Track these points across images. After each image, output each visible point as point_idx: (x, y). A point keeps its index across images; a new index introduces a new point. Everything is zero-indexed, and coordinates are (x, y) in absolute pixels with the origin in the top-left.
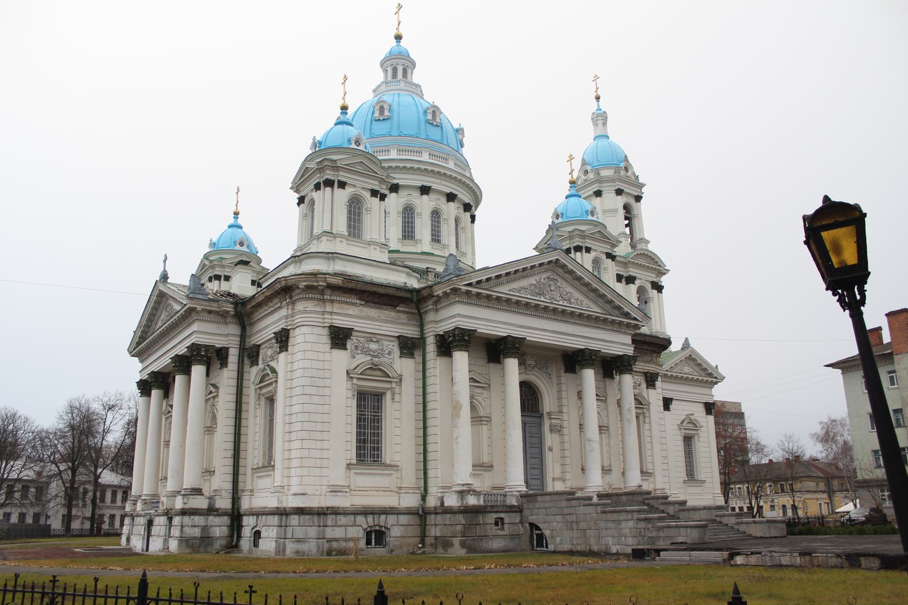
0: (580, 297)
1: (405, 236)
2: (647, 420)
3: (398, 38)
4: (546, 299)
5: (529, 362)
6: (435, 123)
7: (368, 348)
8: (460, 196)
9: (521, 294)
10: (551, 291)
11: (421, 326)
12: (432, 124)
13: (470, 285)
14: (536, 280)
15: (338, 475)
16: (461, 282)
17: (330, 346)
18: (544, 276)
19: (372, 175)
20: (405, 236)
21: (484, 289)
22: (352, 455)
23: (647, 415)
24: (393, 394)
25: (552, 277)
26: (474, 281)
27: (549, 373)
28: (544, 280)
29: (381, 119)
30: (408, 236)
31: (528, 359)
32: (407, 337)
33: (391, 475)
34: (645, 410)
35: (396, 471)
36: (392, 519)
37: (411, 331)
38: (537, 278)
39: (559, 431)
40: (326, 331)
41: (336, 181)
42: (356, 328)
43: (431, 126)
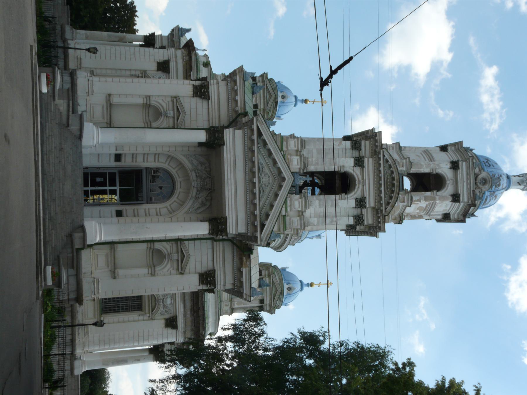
2: (141, 318)
17: (158, 61)
19: (266, 103)
23: (146, 318)
34: (148, 315)
40: (166, 58)
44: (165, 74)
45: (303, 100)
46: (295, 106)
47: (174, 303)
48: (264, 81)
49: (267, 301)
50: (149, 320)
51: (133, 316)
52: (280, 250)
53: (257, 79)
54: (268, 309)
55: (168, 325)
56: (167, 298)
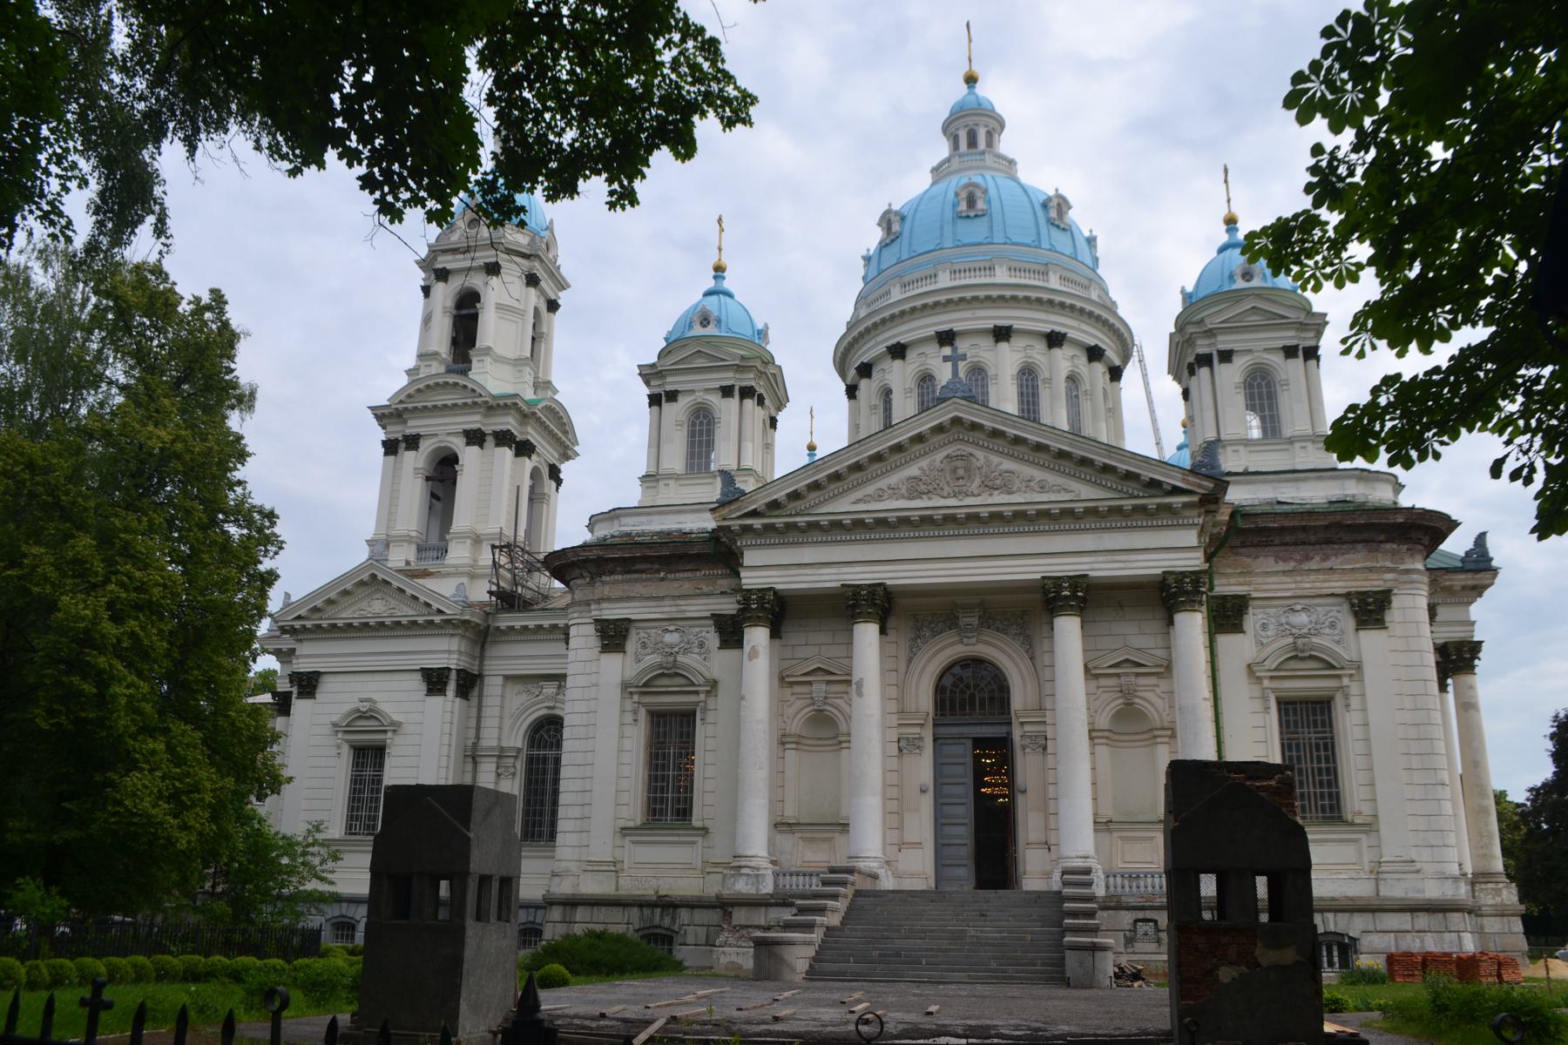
0: (1039, 474)
2: (1355, 702)
3: (971, 80)
5: (963, 621)
6: (972, 214)
8: (1017, 325)
12: (968, 217)
13: (754, 514)
15: (603, 846)
22: (634, 811)
23: (1354, 689)
24: (705, 710)
27: (1028, 632)
31: (961, 615)
32: (724, 616)
33: (694, 843)
34: (1346, 681)
35: (703, 836)
36: (684, 915)
37: (728, 606)
38: (924, 463)
39: (1045, 748)
40: (591, 629)
42: (633, 617)
43: (967, 221)
44: (633, 632)
45: (715, 277)
46: (730, 295)
47: (1303, 601)
48: (661, 372)
49: (1289, 337)
50: (1362, 680)
51: (1347, 723)
52: (1126, 335)
53: (656, 391)
54: (1312, 334)
55: (1378, 620)
56: (1287, 623)
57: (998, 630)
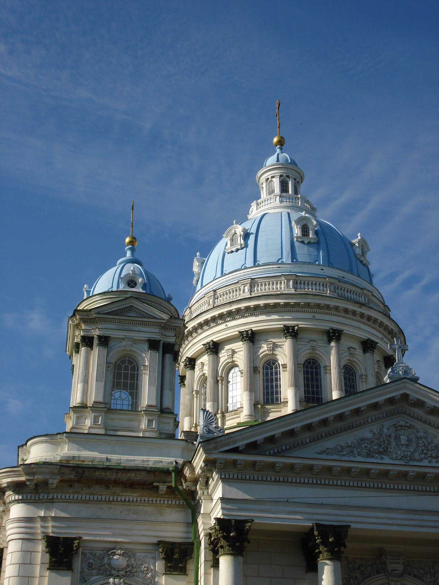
1: (268, 400)
4: (391, 458)
5: (390, 567)
7: (109, 564)
8: (347, 330)
9: (343, 455)
10: (402, 445)
11: (194, 522)
13: (235, 450)
14: (371, 431)
16: (216, 448)
18: (388, 423)
20: (268, 400)
21: (266, 455)
25: (402, 423)
26: (241, 444)
28: (388, 429)
29: (234, 249)
30: (272, 399)
38: (375, 428)
41: (96, 337)
48: (95, 318)
57: (415, 576)
